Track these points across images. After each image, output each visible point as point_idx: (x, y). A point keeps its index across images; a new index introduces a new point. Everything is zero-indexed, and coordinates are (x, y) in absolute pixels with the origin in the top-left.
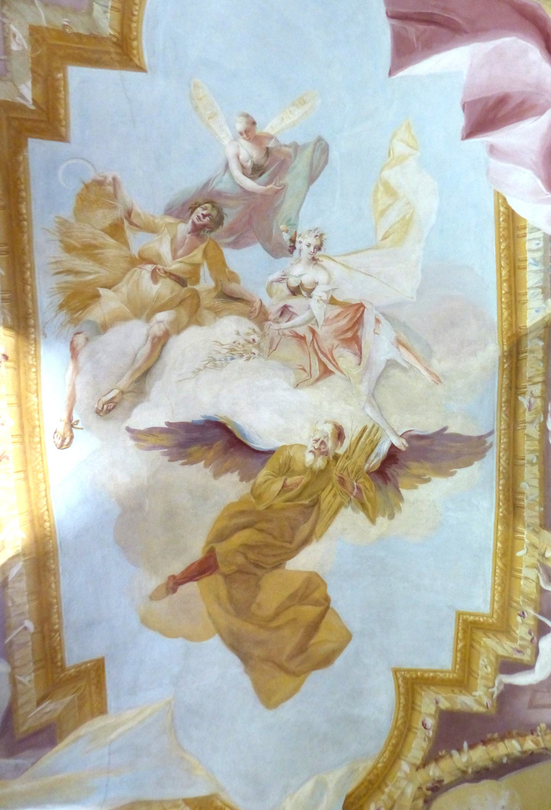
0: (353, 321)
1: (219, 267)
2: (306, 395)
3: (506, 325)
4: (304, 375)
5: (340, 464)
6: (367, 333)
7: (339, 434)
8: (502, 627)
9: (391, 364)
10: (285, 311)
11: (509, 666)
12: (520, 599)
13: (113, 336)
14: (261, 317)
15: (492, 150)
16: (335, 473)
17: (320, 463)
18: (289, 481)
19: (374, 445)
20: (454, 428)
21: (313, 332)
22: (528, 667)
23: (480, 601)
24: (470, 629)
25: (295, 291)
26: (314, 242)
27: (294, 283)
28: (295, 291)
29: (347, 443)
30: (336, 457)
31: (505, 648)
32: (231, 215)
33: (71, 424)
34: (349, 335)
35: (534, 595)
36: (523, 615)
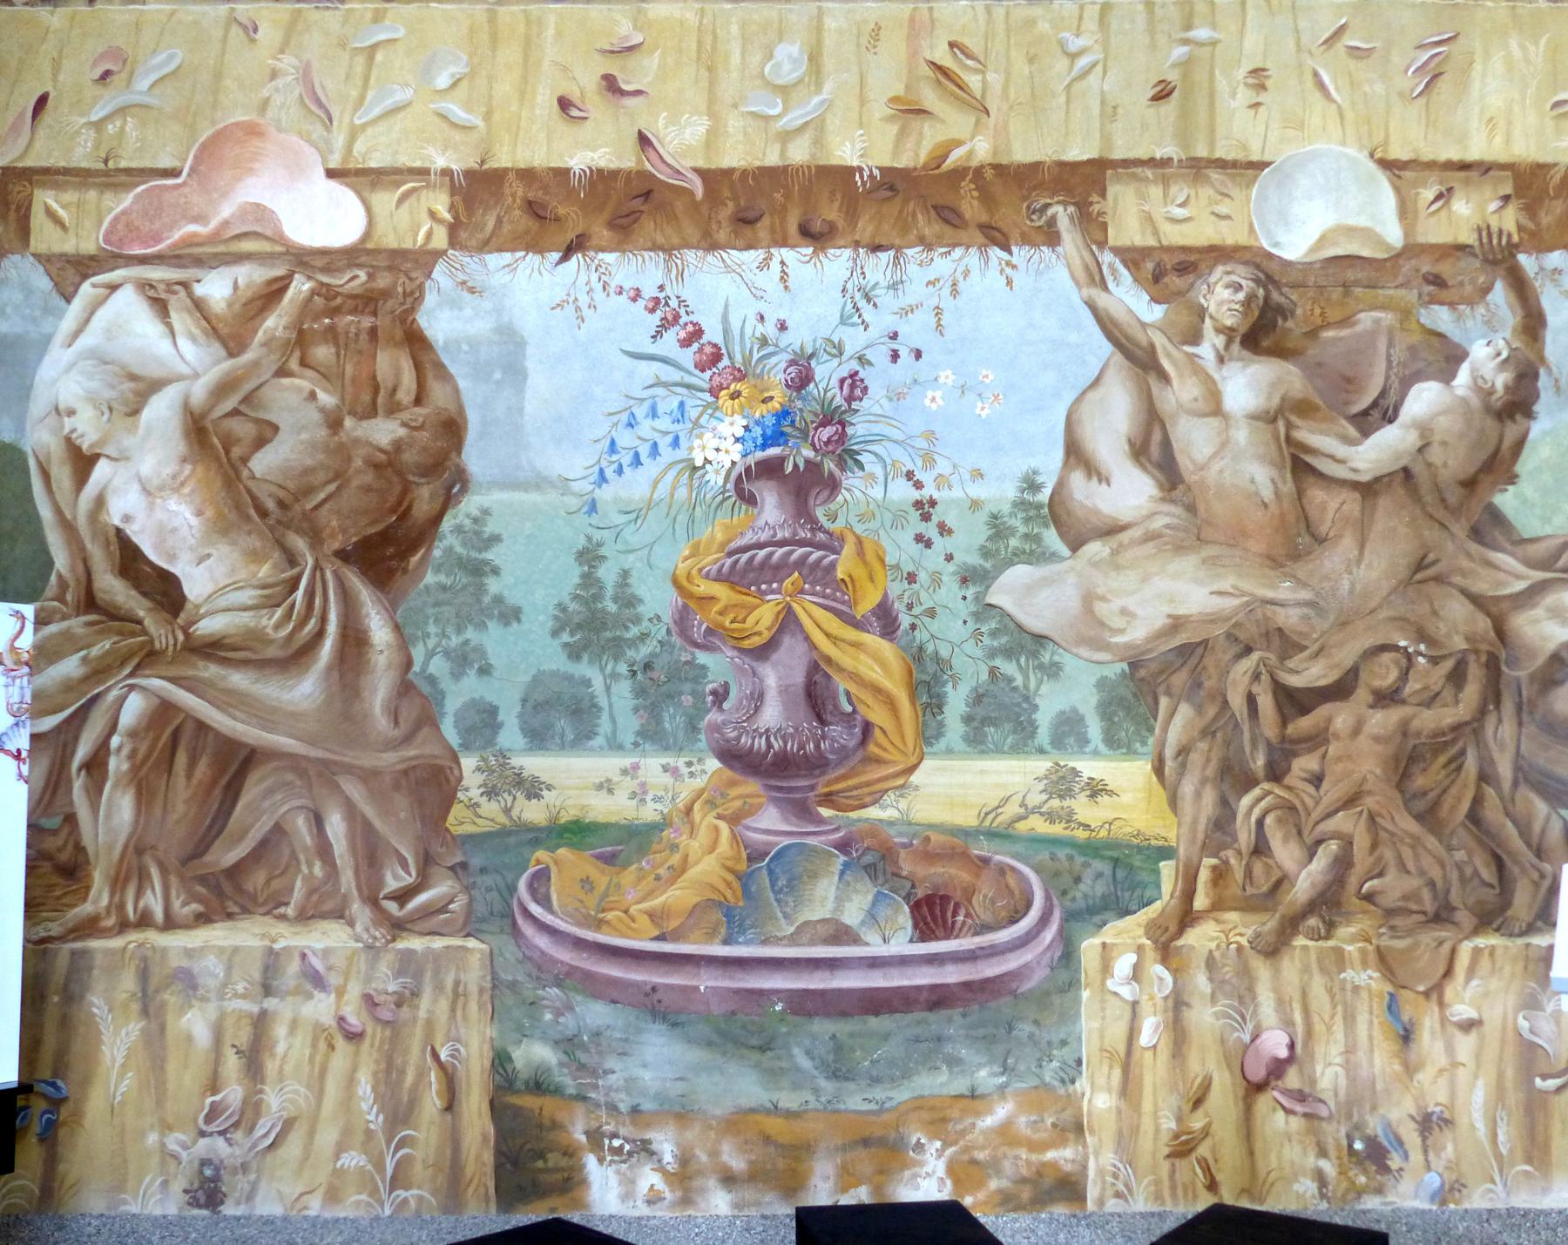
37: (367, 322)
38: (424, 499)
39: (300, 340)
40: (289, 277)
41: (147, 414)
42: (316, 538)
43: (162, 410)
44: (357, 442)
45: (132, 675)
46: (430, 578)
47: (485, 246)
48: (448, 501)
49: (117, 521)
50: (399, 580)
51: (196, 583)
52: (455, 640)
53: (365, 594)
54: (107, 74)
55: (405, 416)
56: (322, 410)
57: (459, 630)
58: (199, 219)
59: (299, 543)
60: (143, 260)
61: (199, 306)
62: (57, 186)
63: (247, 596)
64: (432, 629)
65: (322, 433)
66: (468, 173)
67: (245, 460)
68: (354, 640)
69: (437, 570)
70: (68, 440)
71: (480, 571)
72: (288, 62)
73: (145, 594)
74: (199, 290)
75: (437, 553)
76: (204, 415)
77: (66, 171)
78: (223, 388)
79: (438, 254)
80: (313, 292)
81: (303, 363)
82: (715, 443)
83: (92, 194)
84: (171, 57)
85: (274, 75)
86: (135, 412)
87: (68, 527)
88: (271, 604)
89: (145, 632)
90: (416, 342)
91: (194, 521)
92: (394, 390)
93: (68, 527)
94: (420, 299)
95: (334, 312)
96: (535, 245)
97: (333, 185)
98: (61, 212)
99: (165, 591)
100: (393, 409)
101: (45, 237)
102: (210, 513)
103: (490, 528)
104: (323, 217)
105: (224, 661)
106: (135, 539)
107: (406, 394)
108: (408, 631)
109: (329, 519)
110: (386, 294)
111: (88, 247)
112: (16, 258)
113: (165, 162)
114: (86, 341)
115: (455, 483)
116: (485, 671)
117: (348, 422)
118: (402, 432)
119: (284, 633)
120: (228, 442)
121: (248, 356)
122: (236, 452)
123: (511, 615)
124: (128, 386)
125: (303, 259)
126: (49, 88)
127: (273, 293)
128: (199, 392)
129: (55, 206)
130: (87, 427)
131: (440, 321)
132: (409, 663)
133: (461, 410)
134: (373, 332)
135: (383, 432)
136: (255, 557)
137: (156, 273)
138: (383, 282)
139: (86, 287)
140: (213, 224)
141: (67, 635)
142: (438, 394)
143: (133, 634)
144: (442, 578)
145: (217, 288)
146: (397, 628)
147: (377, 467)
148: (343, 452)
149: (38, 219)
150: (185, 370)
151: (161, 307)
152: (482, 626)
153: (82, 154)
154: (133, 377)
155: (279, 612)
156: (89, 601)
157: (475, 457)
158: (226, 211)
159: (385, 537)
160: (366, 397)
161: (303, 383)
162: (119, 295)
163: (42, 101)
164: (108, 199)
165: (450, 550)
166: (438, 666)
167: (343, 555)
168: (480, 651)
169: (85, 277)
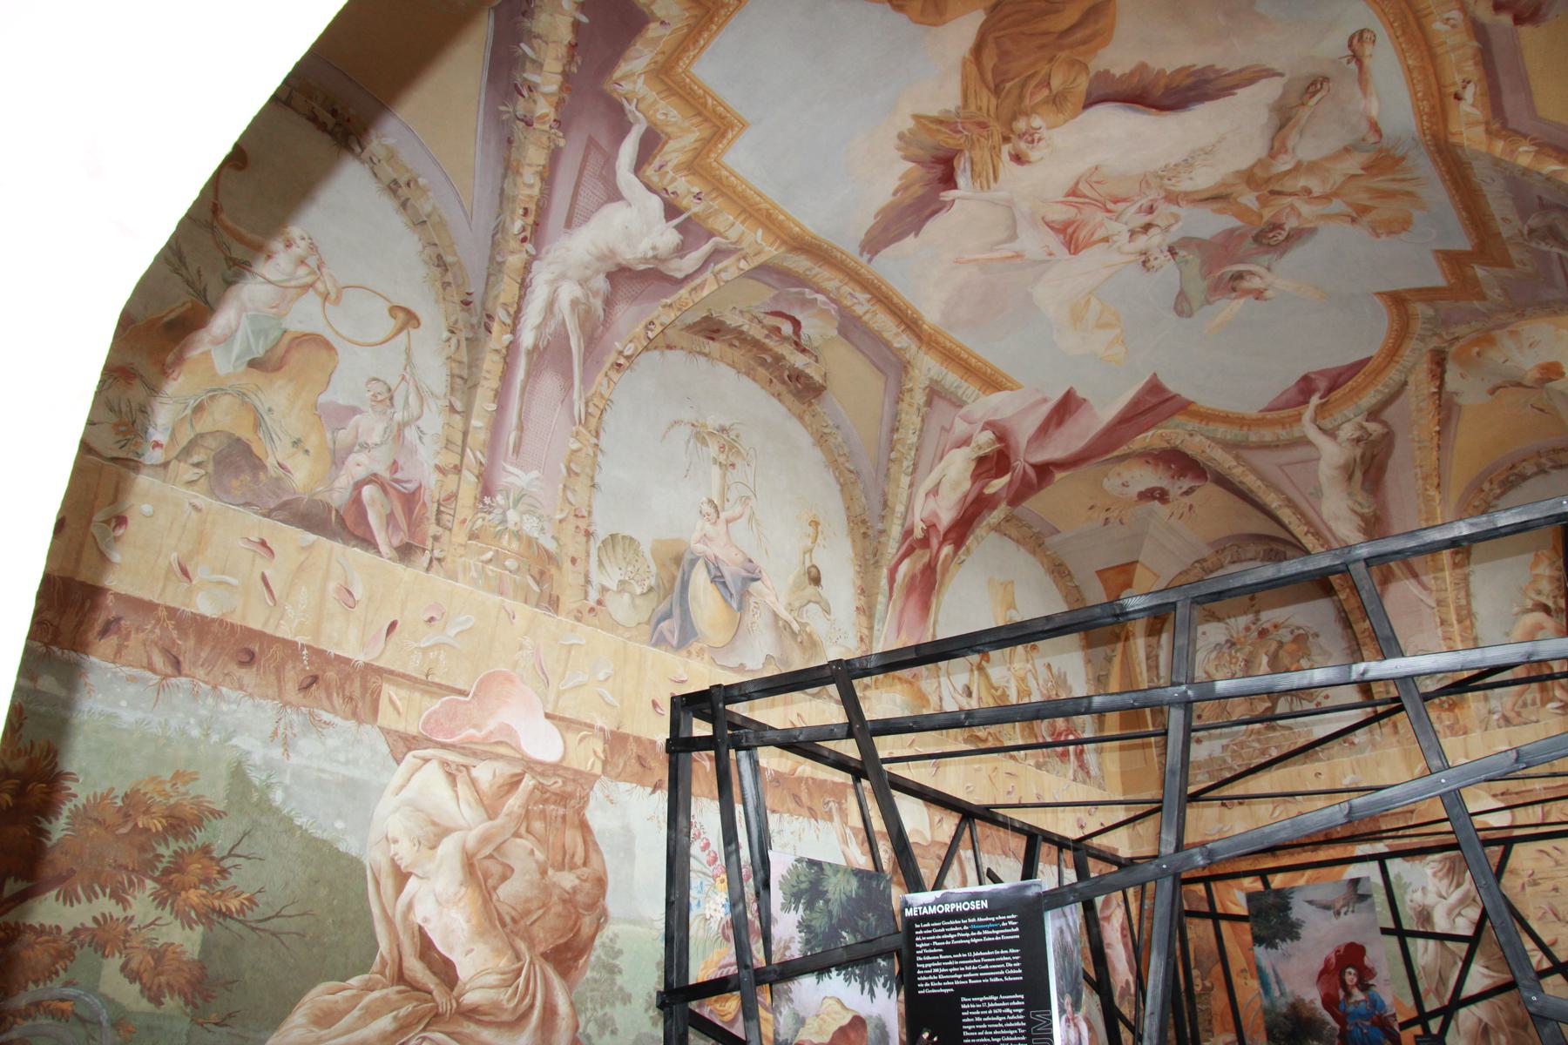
0: (1071, 237)
1: (1242, 213)
2: (1080, 167)
3: (941, 339)
4: (1094, 178)
5: (997, 138)
6: (1054, 242)
7: (1018, 158)
8: (695, 166)
9: (1013, 237)
10: (1151, 210)
11: (651, 144)
12: (715, 204)
13: (1331, 144)
14: (1172, 198)
15: (1045, 400)
16: (997, 129)
17: (1021, 125)
18: (1046, 92)
19: (975, 175)
20: (910, 241)
21: (1109, 211)
22: (638, 168)
23: (740, 159)
24: (719, 125)
25: (1147, 227)
26: (1152, 263)
27: (1153, 231)
28: (1147, 227)
29: (1005, 156)
30: (1006, 139)
31: (674, 153)
32: (1248, 244)
33: (1357, 58)
34: (1070, 230)
35: (713, 224)
36: (698, 197)
37: (561, 811)
38: (587, 923)
39: (527, 816)
40: (522, 775)
41: (441, 850)
42: (531, 947)
43: (449, 847)
44: (554, 884)
45: (424, 1030)
46: (589, 974)
47: (618, 777)
48: (598, 927)
49: (419, 921)
50: (574, 973)
51: (464, 970)
52: (600, 1013)
53: (556, 981)
54: (431, 619)
55: (579, 872)
56: (537, 862)
57: (602, 1007)
58: (475, 726)
59: (522, 946)
60: (444, 746)
61: (473, 782)
62: (397, 685)
63: (493, 979)
64: (589, 1005)
65: (537, 876)
66: (612, 733)
67: (495, 888)
68: (550, 1011)
69: (593, 969)
70: (393, 860)
71: (613, 970)
72: (528, 641)
73: (434, 973)
74: (475, 772)
75: (593, 958)
76: (474, 855)
77: (404, 676)
78: (485, 840)
79: (597, 777)
80: (535, 787)
81: (528, 831)
82: (714, 907)
83: (417, 695)
84: (468, 620)
85: (521, 648)
86: (433, 848)
87: (389, 921)
88: (506, 985)
89: (433, 1000)
90: (584, 827)
91: (465, 926)
92: (573, 856)
93: (389, 921)
94: (587, 802)
95: (545, 801)
96: (641, 782)
97: (548, 722)
98: (398, 703)
99: (446, 972)
100: (573, 867)
101: (386, 717)
102: (474, 922)
103: (617, 946)
104: (544, 744)
105: (478, 1022)
106: (430, 934)
107: (579, 859)
108: (578, 1006)
109: (539, 932)
110: (571, 796)
111: (413, 730)
112: (368, 727)
113: (460, 686)
114: (405, 794)
115: (602, 919)
116: (614, 1032)
117: (550, 872)
118: (577, 882)
119: (512, 1005)
120: (486, 876)
121: (499, 821)
122: (491, 882)
123: (627, 999)
124: (431, 828)
125: (531, 765)
126: (397, 618)
127: (514, 783)
128: (472, 839)
129: (395, 697)
130: (405, 852)
131: (597, 817)
132: (577, 1027)
133: (605, 873)
134: (564, 817)
135: (568, 880)
136: (499, 952)
137: (451, 757)
138: (569, 788)
139: (409, 756)
140: (484, 732)
141: (385, 999)
142: (593, 857)
143: (426, 1001)
144: (595, 974)
145: (486, 773)
146: (572, 1004)
147: (564, 901)
148: (546, 889)
149: (384, 704)
150: (462, 822)
151: (452, 778)
152: (613, 1005)
153: (413, 667)
154: (434, 824)
155: (510, 991)
156: (400, 977)
157: (612, 902)
158: (492, 725)
159: (567, 946)
160: (559, 858)
161: (526, 843)
162: (428, 765)
163: (393, 625)
164: (427, 700)
165: (599, 957)
166: (592, 1029)
167: (545, 956)
168: (612, 1019)
169: (410, 749)
